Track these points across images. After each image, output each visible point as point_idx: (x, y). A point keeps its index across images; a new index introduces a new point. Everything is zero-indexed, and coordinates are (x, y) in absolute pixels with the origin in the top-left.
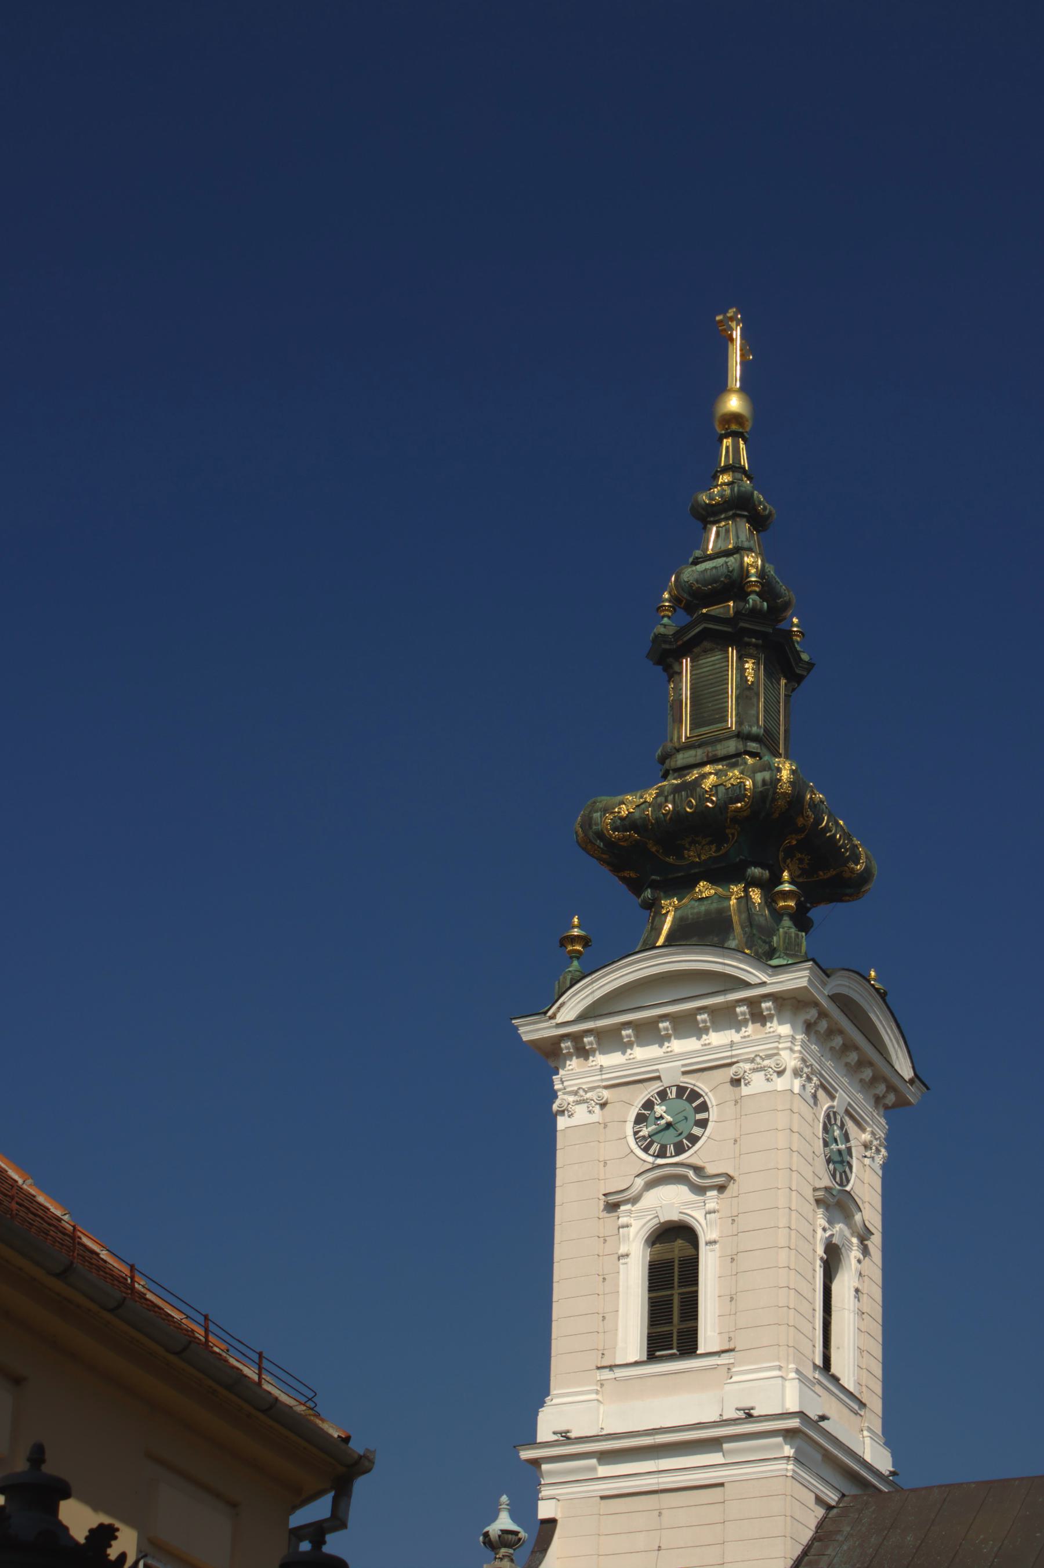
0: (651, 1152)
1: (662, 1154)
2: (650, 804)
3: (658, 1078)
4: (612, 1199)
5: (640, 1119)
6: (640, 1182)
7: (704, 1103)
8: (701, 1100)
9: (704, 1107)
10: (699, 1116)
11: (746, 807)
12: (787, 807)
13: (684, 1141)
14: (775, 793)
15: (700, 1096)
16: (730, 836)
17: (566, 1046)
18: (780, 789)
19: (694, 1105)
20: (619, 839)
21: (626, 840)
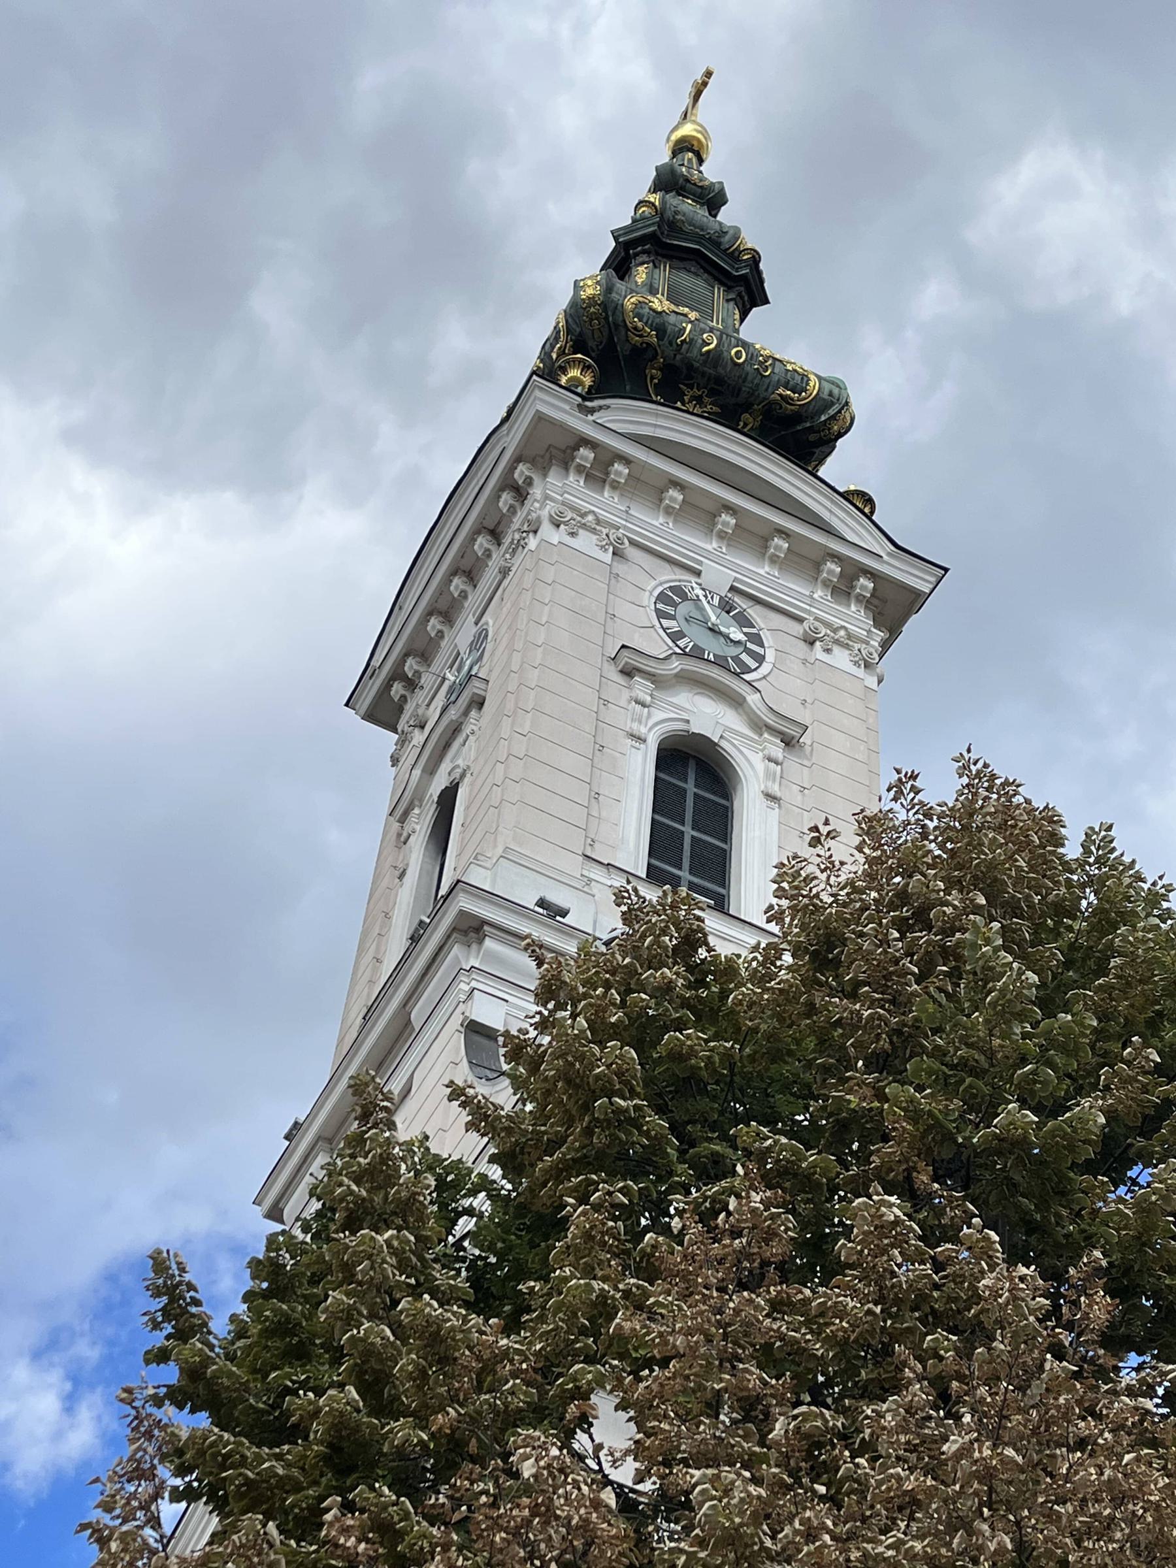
0: (681, 643)
1: (697, 654)
2: (691, 322)
3: (698, 574)
4: (626, 658)
5: (662, 597)
6: (676, 665)
9: (757, 639)
10: (749, 645)
14: (840, 412)
17: (585, 455)
20: (636, 328)
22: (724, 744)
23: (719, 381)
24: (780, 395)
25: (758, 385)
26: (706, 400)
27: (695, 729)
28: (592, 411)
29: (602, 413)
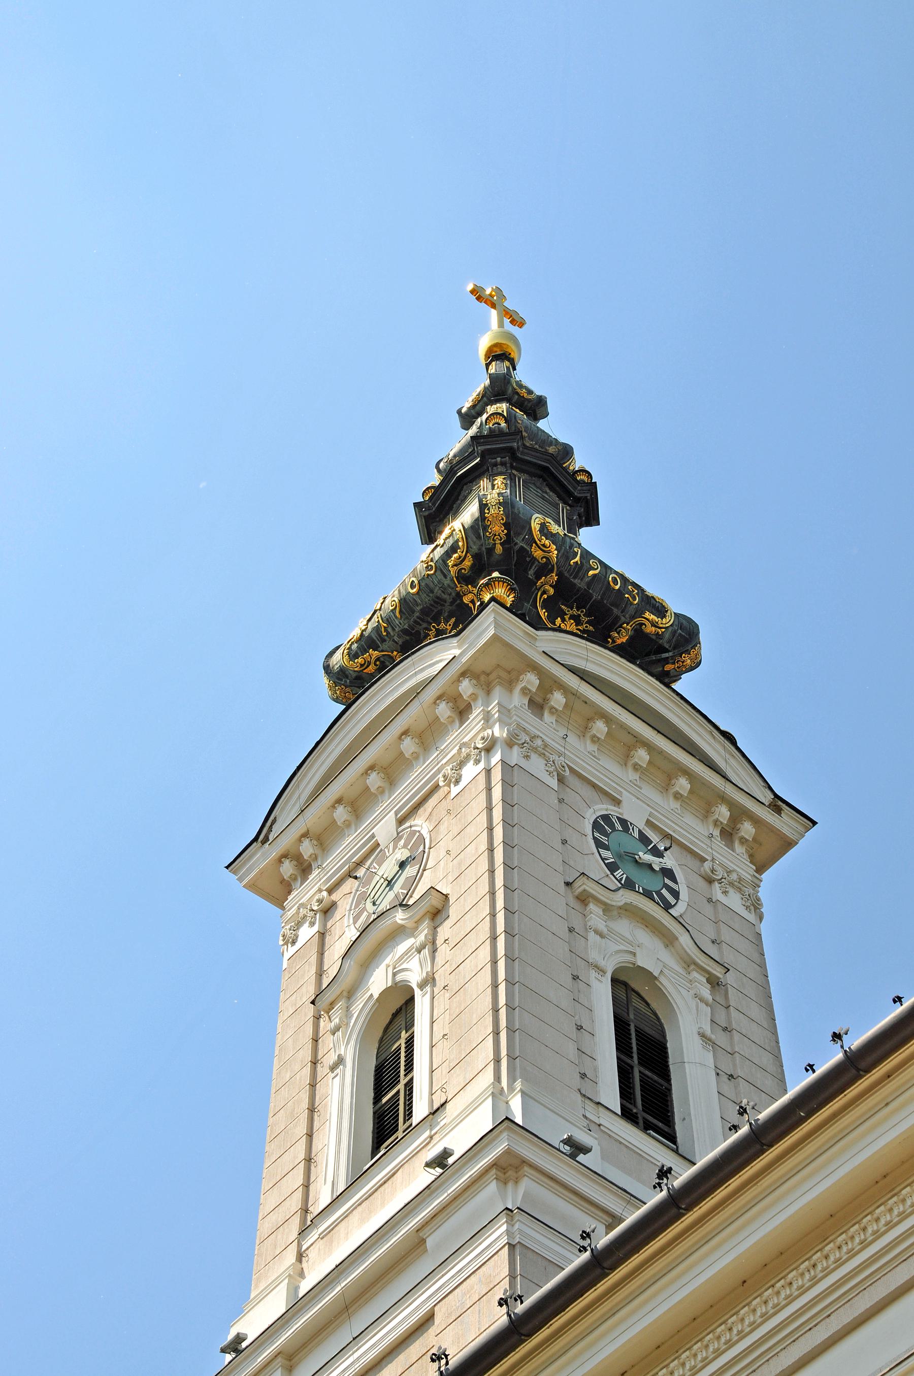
7: (421, 835)
8: (418, 834)
11: (464, 553)
12: (506, 531)
13: (401, 891)
15: (415, 832)
16: (471, 605)
18: (488, 513)
19: (409, 847)
20: (362, 665)
21: (369, 663)
22: (399, 978)
23: (425, 612)
24: (452, 567)
25: (439, 582)
26: (442, 626)
27: (376, 996)
28: (266, 839)
29: (275, 827)
